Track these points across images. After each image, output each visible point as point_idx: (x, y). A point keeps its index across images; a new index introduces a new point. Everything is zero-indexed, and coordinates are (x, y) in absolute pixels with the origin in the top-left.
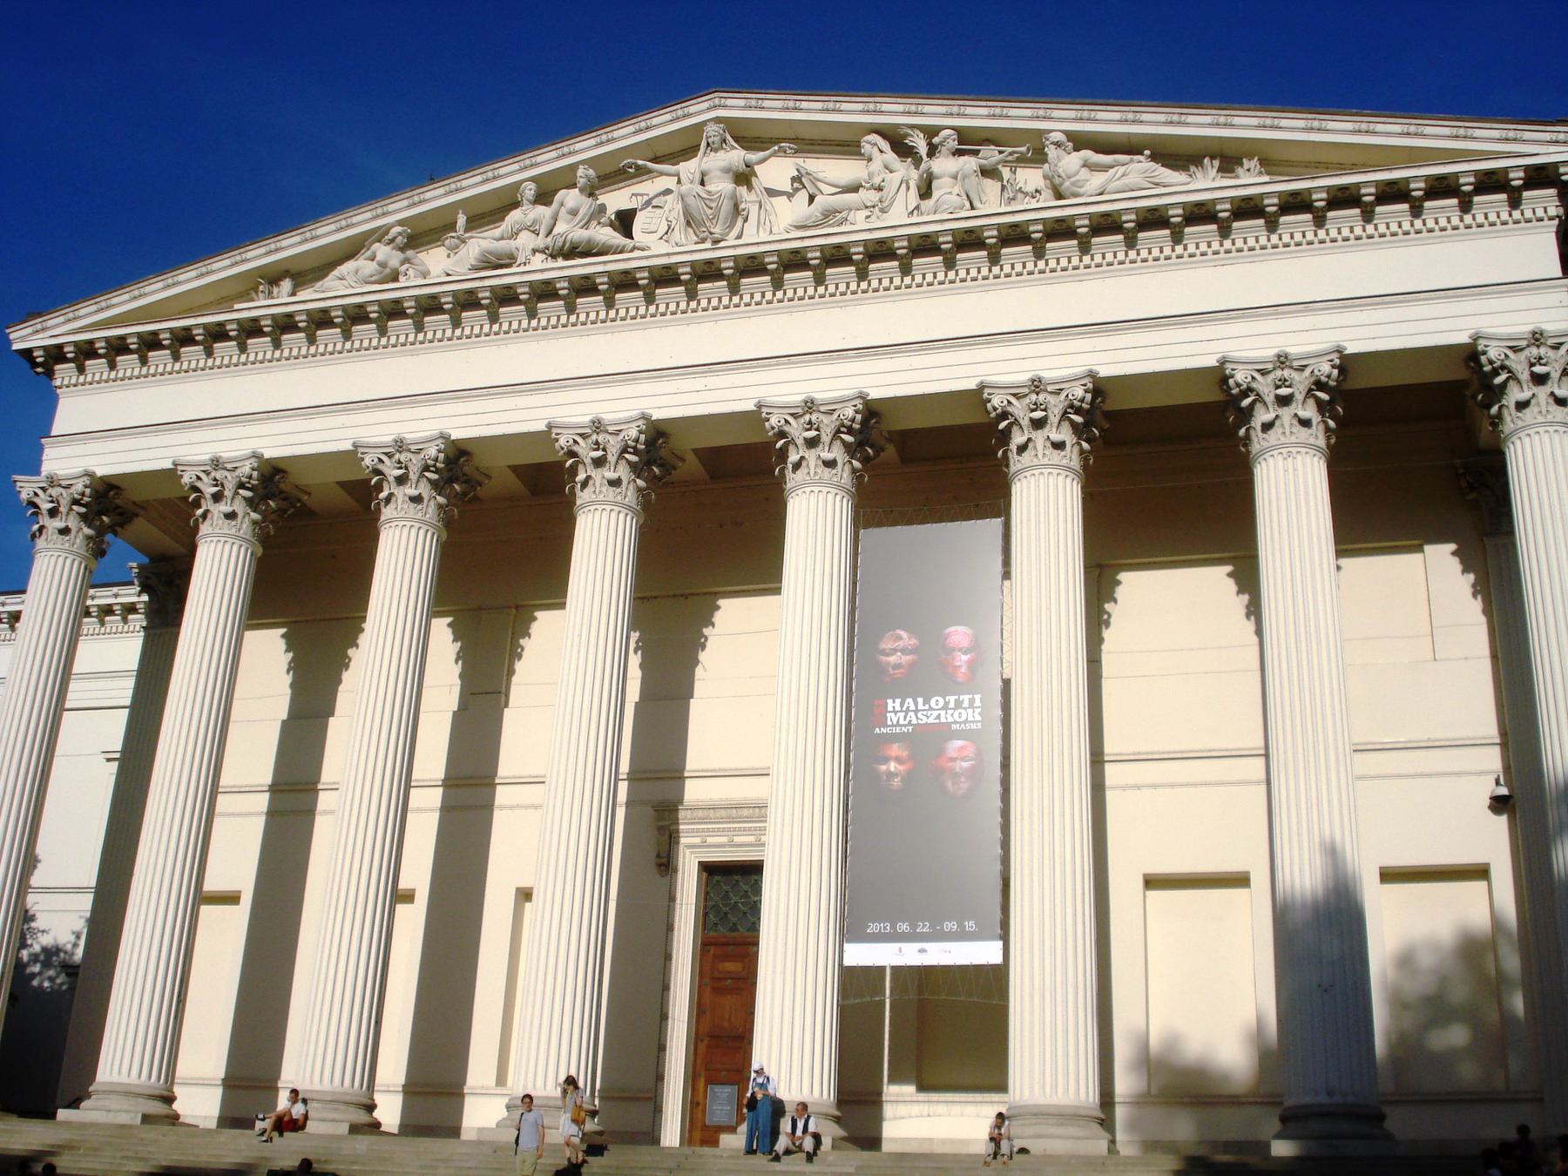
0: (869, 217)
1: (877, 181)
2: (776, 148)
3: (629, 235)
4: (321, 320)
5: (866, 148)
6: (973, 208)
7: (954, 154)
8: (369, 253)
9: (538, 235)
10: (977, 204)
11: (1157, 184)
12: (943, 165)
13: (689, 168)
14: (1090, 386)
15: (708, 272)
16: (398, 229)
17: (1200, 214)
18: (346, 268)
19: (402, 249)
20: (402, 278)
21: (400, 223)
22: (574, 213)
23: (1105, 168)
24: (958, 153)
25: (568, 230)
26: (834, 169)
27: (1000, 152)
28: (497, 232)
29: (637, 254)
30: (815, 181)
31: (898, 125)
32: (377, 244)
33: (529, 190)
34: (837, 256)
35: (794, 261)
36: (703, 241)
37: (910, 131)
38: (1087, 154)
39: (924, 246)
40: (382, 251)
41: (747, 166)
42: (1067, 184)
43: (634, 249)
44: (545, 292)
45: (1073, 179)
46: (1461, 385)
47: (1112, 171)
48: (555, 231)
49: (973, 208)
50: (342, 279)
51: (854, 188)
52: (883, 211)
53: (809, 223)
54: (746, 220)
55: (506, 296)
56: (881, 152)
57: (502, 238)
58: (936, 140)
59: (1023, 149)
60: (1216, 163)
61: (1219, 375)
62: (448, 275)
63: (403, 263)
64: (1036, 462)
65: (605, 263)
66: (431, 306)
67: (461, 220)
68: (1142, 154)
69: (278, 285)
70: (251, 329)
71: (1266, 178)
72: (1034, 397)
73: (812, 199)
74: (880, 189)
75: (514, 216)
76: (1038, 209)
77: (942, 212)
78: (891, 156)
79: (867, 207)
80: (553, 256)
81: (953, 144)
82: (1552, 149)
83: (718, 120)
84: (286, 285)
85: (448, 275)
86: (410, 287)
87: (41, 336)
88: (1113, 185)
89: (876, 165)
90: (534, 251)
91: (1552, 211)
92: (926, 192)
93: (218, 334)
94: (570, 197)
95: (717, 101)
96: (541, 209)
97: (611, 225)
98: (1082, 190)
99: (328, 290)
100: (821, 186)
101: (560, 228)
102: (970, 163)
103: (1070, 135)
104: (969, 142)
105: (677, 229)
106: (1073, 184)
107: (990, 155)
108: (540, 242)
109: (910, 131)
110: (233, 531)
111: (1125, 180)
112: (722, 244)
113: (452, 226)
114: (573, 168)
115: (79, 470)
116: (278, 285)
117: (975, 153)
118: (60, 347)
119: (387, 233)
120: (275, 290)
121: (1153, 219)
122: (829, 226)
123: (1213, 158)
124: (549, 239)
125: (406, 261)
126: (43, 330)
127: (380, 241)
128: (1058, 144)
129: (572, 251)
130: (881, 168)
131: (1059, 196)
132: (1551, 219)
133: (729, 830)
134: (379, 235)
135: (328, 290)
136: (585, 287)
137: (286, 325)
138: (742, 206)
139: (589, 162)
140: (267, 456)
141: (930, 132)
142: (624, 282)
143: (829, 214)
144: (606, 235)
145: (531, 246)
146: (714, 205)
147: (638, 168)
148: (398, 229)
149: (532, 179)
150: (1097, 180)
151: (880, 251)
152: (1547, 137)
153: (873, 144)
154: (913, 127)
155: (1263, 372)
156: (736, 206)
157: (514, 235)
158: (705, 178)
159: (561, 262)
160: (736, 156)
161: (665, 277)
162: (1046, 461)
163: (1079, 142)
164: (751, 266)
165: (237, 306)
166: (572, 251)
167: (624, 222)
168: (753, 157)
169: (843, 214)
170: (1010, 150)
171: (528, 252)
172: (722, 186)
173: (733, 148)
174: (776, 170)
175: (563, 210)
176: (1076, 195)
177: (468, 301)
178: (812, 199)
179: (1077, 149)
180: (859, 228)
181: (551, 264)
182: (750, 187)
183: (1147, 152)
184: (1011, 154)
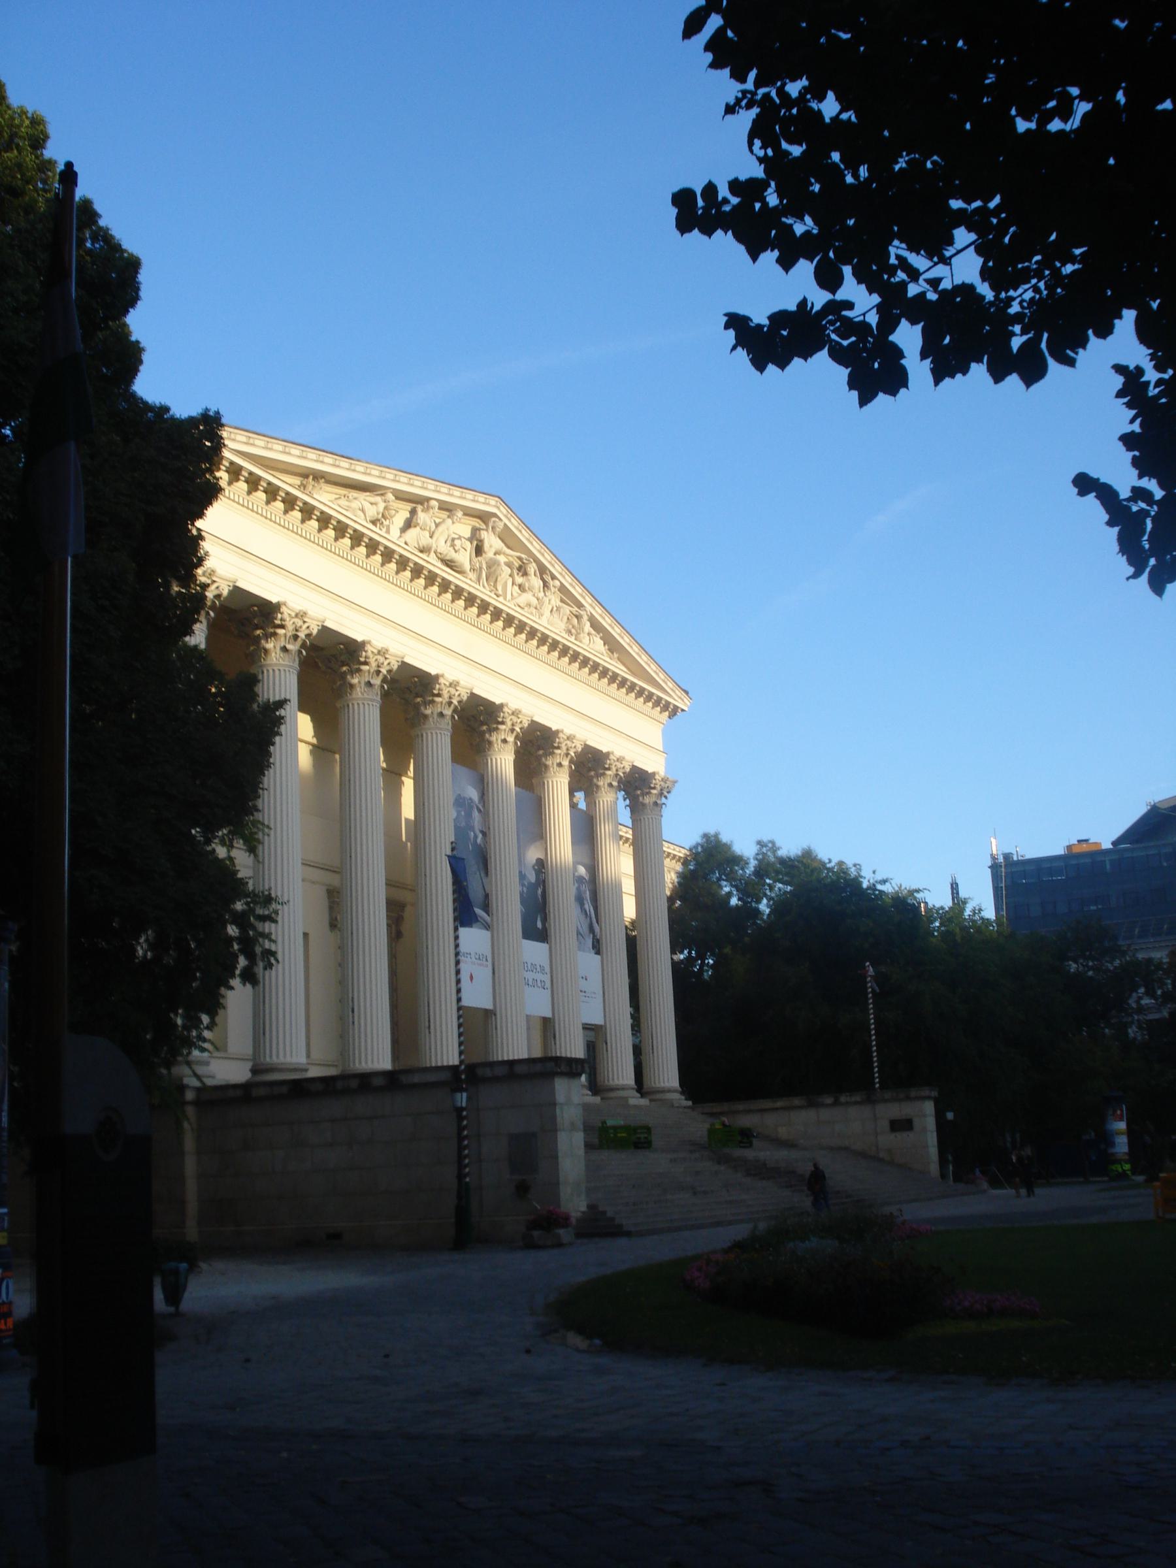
8: (373, 499)
9: (431, 537)
32: (378, 499)
37: (548, 572)
50: (363, 511)
56: (535, 575)
62: (406, 543)
68: (599, 634)
71: (625, 669)
77: (556, 628)
82: (680, 700)
85: (406, 543)
104: (563, 589)
109: (548, 572)
129: (449, 564)
141: (554, 577)
153: (532, 568)
154: (550, 571)
166: (449, 564)
176: (581, 642)
178: (513, 584)
181: (439, 564)
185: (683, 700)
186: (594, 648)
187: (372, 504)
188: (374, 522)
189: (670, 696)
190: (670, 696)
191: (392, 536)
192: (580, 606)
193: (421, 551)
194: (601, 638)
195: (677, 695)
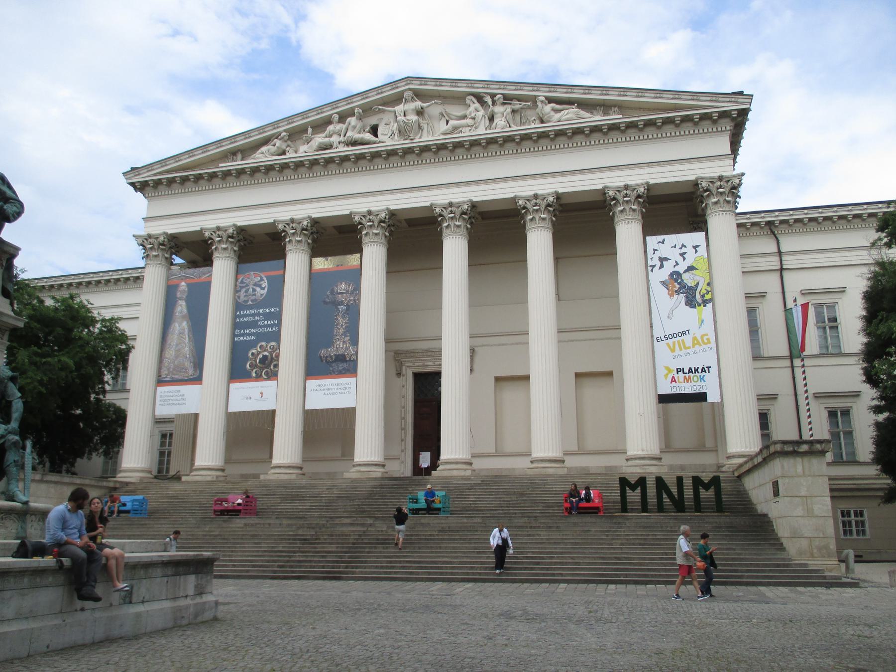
0: (470, 130)
1: (473, 115)
2: (433, 102)
3: (376, 136)
4: (255, 170)
5: (468, 102)
6: (510, 127)
7: (502, 104)
10: (512, 125)
12: (498, 109)
13: (399, 109)
14: (555, 196)
15: (408, 151)
16: (284, 134)
17: (596, 129)
18: (264, 149)
19: (286, 141)
20: (287, 154)
21: (285, 131)
22: (354, 127)
23: (560, 111)
24: (504, 104)
25: (353, 135)
26: (456, 110)
27: (520, 104)
28: (324, 135)
29: (381, 144)
30: (448, 115)
31: (480, 93)
33: (336, 117)
34: (458, 145)
35: (441, 147)
36: (406, 139)
37: (485, 95)
38: (553, 105)
39: (491, 141)
40: (278, 143)
41: (422, 108)
43: (380, 142)
44: (345, 159)
46: (693, 193)
47: (563, 112)
48: (347, 135)
49: (510, 127)
50: (263, 153)
51: (464, 117)
52: (476, 128)
53: (447, 132)
54: (422, 130)
55: (329, 161)
57: (326, 137)
58: (495, 99)
59: (529, 103)
60: (602, 108)
61: (603, 192)
63: (287, 147)
65: (369, 148)
66: (299, 165)
67: (310, 130)
68: (574, 105)
69: (236, 156)
70: (227, 174)
71: (621, 116)
72: (535, 201)
73: (447, 122)
74: (474, 118)
75: (331, 128)
76: (534, 127)
78: (477, 105)
79: (469, 126)
80: (348, 145)
81: (502, 100)
83: (410, 89)
84: (239, 156)
86: (291, 156)
87: (138, 177)
88: (564, 118)
89: (472, 109)
90: (339, 143)
91: (728, 128)
92: (491, 119)
93: (213, 176)
94: (353, 120)
95: (409, 82)
96: (341, 125)
97: (369, 132)
98: (551, 120)
99: (258, 158)
100: (451, 116)
101: (349, 134)
102: (509, 109)
103: (547, 98)
104: (507, 99)
105: (396, 135)
107: (517, 105)
108: (342, 139)
109: (485, 95)
110: (227, 255)
111: (568, 116)
112: (415, 141)
113: (306, 131)
114: (353, 109)
115: (161, 232)
116: (236, 156)
117: (510, 104)
118: (147, 182)
119: (280, 135)
120: (235, 158)
121: (578, 132)
122: (456, 133)
123: (600, 106)
124: (345, 138)
125: (288, 146)
126: (139, 174)
127: (277, 138)
128: (542, 102)
129: (354, 143)
130: (474, 110)
131: (542, 122)
132: (728, 131)
134: (277, 136)
135: (258, 158)
136: (360, 157)
137: (241, 172)
138: (421, 125)
139: (359, 106)
140: (238, 225)
141: (493, 96)
142: (376, 155)
143: (455, 129)
144: (368, 136)
145: (338, 140)
146: (410, 125)
147: (379, 109)
148: (284, 134)
149: (336, 113)
150: (557, 116)
151: (475, 143)
152: (728, 99)
154: (486, 93)
155: (619, 191)
156: (419, 125)
157: (331, 136)
158: (406, 113)
159: (351, 148)
160: (418, 104)
161: (392, 153)
163: (550, 100)
164: (425, 149)
165: (221, 165)
166: (354, 143)
167: (374, 130)
168: (423, 104)
169: (461, 129)
170: (524, 103)
171: (337, 143)
172: (413, 118)
173: (416, 101)
174: (434, 109)
175: (350, 128)
176: (549, 122)
177: (314, 163)
179: (549, 103)
180: (466, 134)
181: (347, 149)
182: (423, 118)
184: (525, 105)
185: (734, 102)
186: (570, 117)
187: (274, 145)
188: (284, 153)
189: (713, 107)
190: (713, 107)
191: (304, 151)
192: (534, 100)
193: (325, 149)
195: (723, 102)
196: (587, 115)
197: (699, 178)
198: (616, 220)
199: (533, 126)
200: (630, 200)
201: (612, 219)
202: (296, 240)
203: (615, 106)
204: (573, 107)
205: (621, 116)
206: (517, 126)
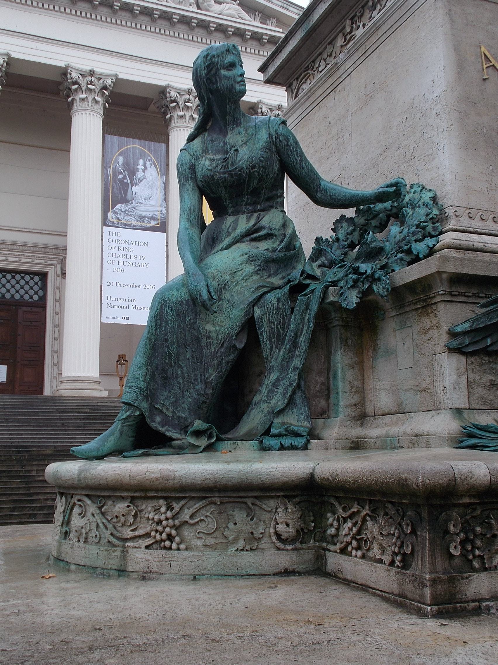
11: (240, 17)
42: (205, 4)
45: (208, 3)
64: (185, 124)
68: (235, 2)
71: (280, 30)
72: (188, 96)
88: (225, 12)
98: (210, 9)
106: (208, 5)
131: (199, 7)
133: (6, 254)
162: (189, 125)
176: (208, 10)
183: (238, 1)
194: (239, 5)
196: (249, 18)
197: (168, 86)
198: (173, 124)
199: (191, 9)
200: (94, 89)
201: (70, 106)
202: (80, 99)
203: (274, 18)
204: (234, 3)
205: (280, 30)
206: (173, 2)
